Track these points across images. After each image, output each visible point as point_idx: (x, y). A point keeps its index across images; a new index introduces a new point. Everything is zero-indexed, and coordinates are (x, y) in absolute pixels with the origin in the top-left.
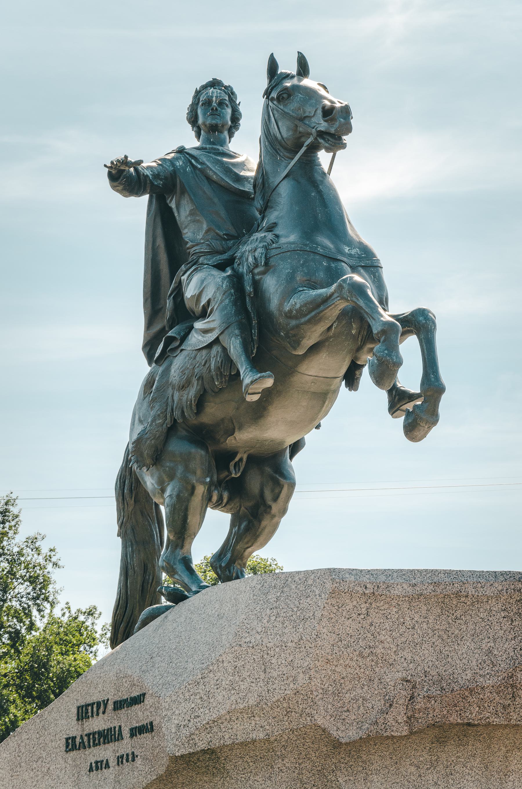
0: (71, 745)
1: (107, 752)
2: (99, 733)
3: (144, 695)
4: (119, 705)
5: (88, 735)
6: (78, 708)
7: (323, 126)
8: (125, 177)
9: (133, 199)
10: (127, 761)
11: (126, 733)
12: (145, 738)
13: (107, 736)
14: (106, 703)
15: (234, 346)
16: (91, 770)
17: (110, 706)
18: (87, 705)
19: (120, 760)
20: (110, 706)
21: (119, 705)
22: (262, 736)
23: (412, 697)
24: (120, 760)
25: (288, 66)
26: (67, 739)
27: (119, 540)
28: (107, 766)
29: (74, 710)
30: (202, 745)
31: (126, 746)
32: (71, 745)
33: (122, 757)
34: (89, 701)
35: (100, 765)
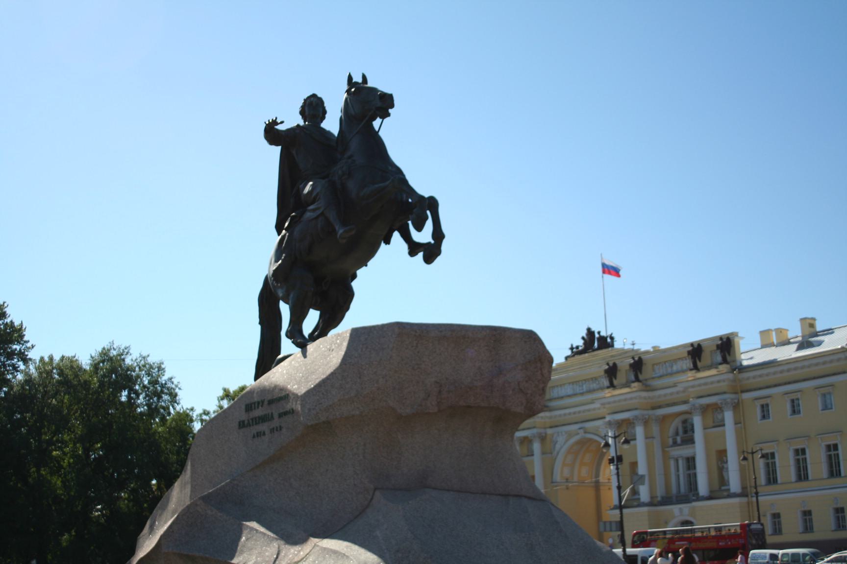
0: (242, 425)
1: (264, 427)
2: (259, 418)
4: (271, 402)
5: (252, 419)
7: (379, 104)
8: (272, 133)
9: (273, 147)
11: (276, 415)
13: (263, 419)
14: (263, 402)
15: (332, 216)
16: (254, 437)
17: (266, 403)
18: (251, 404)
19: (272, 431)
20: (266, 403)
22: (358, 413)
23: (440, 392)
24: (272, 431)
25: (357, 79)
27: (259, 327)
28: (264, 434)
29: (243, 407)
31: (276, 423)
35: (259, 434)
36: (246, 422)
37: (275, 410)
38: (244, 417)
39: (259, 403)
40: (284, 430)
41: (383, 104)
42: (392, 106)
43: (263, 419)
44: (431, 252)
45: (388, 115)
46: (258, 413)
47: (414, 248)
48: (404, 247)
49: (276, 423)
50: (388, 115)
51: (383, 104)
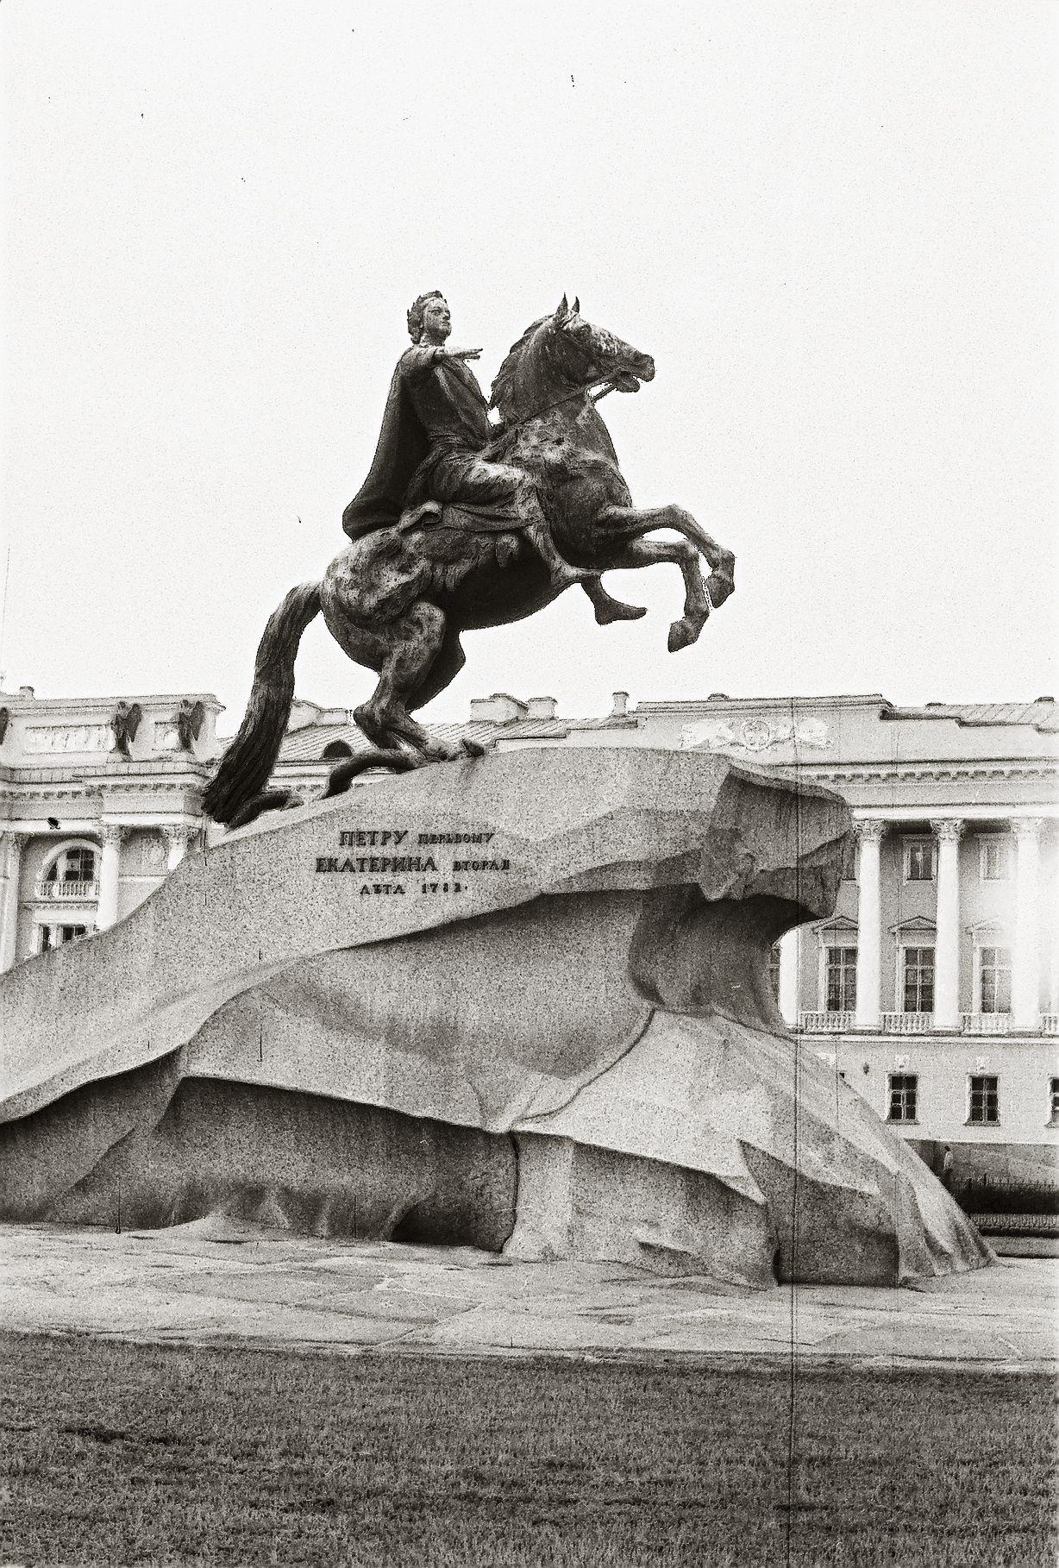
0: (325, 865)
1: (401, 878)
2: (386, 862)
3: (490, 836)
4: (425, 839)
5: (362, 861)
6: (343, 833)
10: (446, 890)
12: (490, 876)
13: (399, 865)
17: (412, 837)
20: (412, 837)
21: (425, 839)
26: (320, 860)
30: (577, 888)
32: (325, 865)
33: (434, 887)
34: (364, 827)
36: (340, 864)
37: (444, 856)
38: (344, 854)
39: (387, 835)
40: (469, 893)
41: (630, 370)
42: (649, 378)
43: (399, 865)
44: (680, 639)
45: (636, 388)
46: (378, 851)
47: (608, 611)
48: (590, 607)
49: (445, 874)
50: (636, 388)
51: (630, 370)
